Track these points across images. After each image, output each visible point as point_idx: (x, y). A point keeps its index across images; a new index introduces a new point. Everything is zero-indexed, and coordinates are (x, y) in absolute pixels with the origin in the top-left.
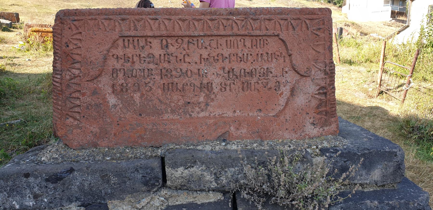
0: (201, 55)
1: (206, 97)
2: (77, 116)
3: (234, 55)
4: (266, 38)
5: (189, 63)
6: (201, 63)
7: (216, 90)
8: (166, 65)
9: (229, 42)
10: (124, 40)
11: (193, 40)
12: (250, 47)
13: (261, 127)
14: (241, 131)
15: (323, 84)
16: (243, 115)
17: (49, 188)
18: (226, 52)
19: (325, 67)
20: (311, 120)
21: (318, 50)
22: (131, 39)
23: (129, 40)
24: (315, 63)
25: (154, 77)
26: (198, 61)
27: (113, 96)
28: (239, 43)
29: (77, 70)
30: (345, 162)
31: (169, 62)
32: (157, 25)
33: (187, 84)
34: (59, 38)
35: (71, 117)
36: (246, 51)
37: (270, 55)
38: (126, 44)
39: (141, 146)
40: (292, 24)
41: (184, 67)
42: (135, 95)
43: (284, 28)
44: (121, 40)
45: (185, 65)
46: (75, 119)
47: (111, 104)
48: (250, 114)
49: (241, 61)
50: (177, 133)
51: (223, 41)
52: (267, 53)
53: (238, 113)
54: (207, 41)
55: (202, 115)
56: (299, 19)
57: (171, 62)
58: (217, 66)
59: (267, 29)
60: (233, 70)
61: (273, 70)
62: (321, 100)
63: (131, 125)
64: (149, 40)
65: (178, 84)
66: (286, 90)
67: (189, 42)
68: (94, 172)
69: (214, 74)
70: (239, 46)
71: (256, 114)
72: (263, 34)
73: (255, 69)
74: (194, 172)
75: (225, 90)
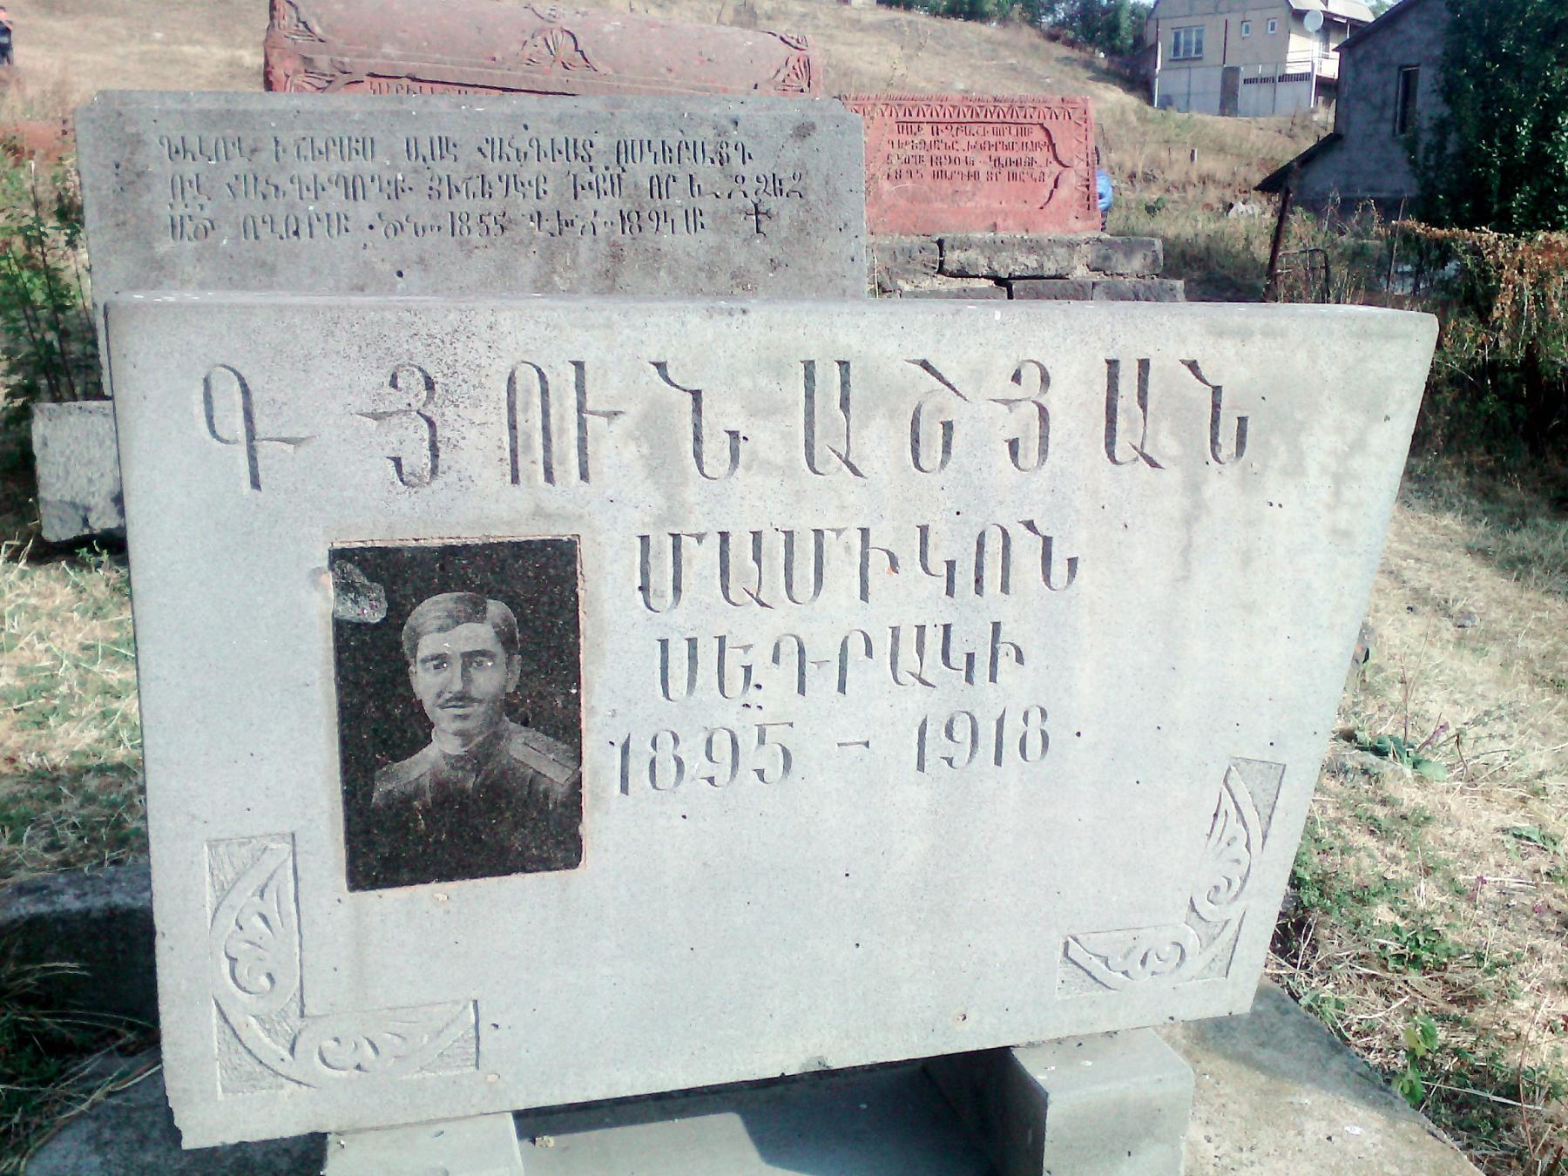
18: (993, 139)
41: (953, 154)
51: (989, 128)
54: (975, 127)
55: (969, 205)
66: (1050, 182)
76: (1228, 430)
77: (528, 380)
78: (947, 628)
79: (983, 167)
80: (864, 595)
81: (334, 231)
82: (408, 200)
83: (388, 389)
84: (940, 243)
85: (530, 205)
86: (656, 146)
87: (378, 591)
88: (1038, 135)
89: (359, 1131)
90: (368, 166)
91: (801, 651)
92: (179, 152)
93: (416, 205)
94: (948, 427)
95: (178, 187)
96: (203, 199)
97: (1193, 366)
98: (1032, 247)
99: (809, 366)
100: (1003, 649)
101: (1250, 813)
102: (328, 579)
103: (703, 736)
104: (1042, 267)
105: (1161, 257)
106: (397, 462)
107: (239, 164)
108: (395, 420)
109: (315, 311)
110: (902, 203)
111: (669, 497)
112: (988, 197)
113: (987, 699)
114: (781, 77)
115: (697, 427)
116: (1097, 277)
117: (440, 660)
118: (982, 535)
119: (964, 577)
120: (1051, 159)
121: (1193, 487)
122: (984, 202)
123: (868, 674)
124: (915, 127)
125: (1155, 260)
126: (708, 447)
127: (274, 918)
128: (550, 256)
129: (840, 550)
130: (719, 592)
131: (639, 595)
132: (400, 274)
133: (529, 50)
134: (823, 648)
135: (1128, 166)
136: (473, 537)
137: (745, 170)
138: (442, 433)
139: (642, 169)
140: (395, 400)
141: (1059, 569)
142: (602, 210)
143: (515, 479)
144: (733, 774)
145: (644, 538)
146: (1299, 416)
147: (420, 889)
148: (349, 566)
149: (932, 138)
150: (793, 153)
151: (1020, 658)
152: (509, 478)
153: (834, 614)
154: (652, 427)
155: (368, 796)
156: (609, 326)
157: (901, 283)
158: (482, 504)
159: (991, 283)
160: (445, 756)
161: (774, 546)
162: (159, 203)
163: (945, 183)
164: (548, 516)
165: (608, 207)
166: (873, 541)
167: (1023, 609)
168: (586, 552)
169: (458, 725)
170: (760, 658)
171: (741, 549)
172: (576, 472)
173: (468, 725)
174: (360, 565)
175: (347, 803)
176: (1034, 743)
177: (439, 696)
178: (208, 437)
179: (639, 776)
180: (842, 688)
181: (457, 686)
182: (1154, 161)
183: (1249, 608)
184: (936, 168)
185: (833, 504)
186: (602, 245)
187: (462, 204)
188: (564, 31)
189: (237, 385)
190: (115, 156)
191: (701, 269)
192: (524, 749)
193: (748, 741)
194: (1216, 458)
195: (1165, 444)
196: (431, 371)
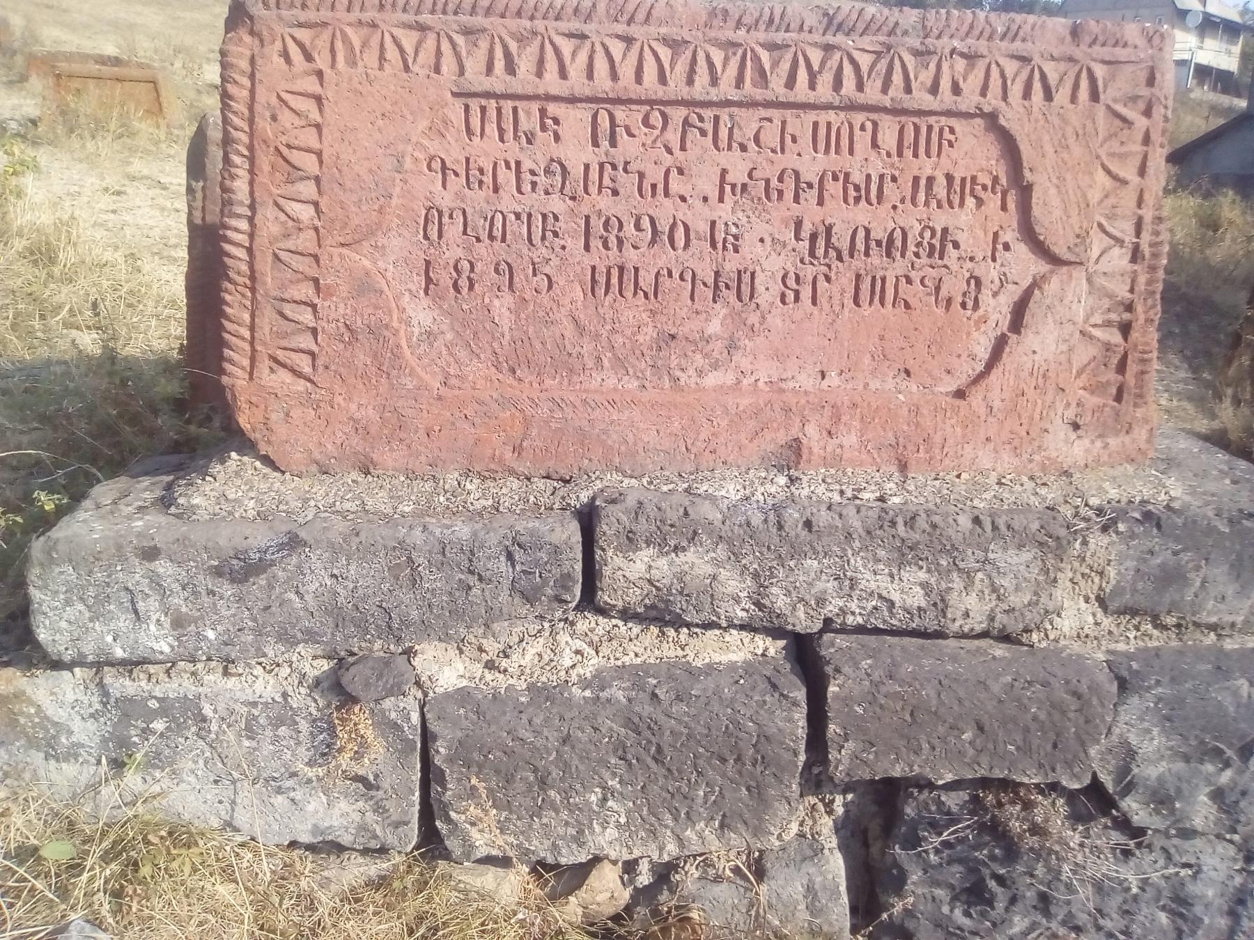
0: (724, 172)
1: (729, 321)
2: (302, 364)
3: (835, 178)
4: (953, 122)
5: (683, 199)
6: (721, 200)
7: (763, 297)
8: (605, 202)
9: (822, 131)
10: (467, 108)
11: (701, 119)
12: (894, 151)
13: (905, 428)
14: (838, 441)
15: (1123, 292)
16: (850, 386)
17: (221, 598)
18: (811, 165)
19: (1138, 235)
20: (1070, 414)
21: (1122, 174)
22: (493, 104)
23: (483, 109)
24: (1108, 217)
25: (562, 242)
26: (714, 195)
27: (426, 302)
28: (857, 132)
29: (304, 206)
30: (1175, 553)
31: (615, 193)
32: (583, 57)
33: (670, 274)
34: (242, 86)
35: (284, 366)
36: (876, 167)
37: (957, 182)
38: (476, 122)
39: (512, 472)
40: (1043, 77)
41: (665, 211)
42: (496, 302)
43: (1016, 90)
44: (458, 105)
45: (667, 202)
46: (297, 373)
47: (416, 331)
48: (874, 384)
49: (857, 200)
50: (630, 438)
51: (801, 124)
52: (949, 178)
53: (833, 379)
54: (749, 122)
55: (712, 379)
56: (1071, 59)
57: (622, 191)
58: (774, 214)
59: (956, 90)
60: (829, 230)
61: (961, 237)
62: (1108, 347)
63: (481, 403)
64: (552, 108)
65: (641, 273)
66: (997, 309)
67: (686, 123)
68: (367, 552)
69: (762, 240)
70: (857, 146)
71: (890, 384)
72: (945, 107)
73: (903, 229)
74: (686, 568)
75: (797, 299)
84: (588, 519)
88: (974, 153)
110: (477, 370)
112: (778, 356)
116: (1131, 640)
120: (1009, 236)
122: (766, 371)
124: (529, 122)
149: (590, 156)
163: (632, 311)
184: (600, 258)
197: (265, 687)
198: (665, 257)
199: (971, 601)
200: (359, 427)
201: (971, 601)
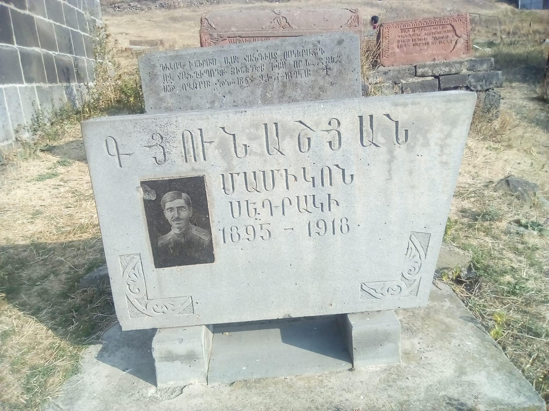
8: (414, 37)
18: (434, 31)
36: (440, 30)
41: (420, 37)
54: (427, 28)
66: (454, 43)
76: (402, 134)
77: (187, 134)
78: (314, 196)
79: (430, 40)
80: (288, 188)
81: (206, 86)
82: (226, 76)
83: (152, 140)
85: (259, 74)
86: (296, 52)
87: (153, 192)
88: (449, 28)
89: (165, 328)
90: (214, 67)
91: (270, 204)
92: (165, 68)
93: (228, 77)
94: (309, 139)
95: (165, 77)
96: (171, 81)
97: (388, 116)
98: (447, 65)
99: (266, 125)
100: (332, 202)
101: (419, 248)
102: (141, 189)
103: (245, 228)
104: (450, 71)
105: (494, 63)
106: (155, 158)
107: (180, 70)
108: (154, 147)
109: (131, 121)
110: (403, 55)
111: (228, 164)
113: (328, 216)
114: (349, 23)
115: (235, 144)
116: (470, 73)
117: (171, 209)
118: (322, 169)
119: (318, 181)
120: (454, 35)
121: (391, 152)
123: (291, 210)
125: (492, 64)
126: (238, 149)
127: (138, 275)
128: (265, 87)
129: (279, 176)
130: (245, 188)
131: (223, 190)
132: (224, 97)
133: (272, 24)
134: (277, 202)
135: (507, 30)
136: (176, 176)
137: (322, 56)
138: (166, 150)
139: (291, 60)
140: (154, 143)
141: (348, 179)
142: (280, 73)
143: (186, 161)
144: (254, 238)
145: (223, 175)
146: (426, 128)
147: (174, 268)
148: (146, 186)
150: (337, 49)
151: (338, 204)
152: (185, 161)
153: (279, 193)
154: (222, 146)
155: (157, 244)
156: (208, 118)
157: (402, 81)
158: (179, 168)
159: (433, 78)
160: (176, 234)
161: (260, 175)
162: (160, 82)
163: (417, 47)
164: (196, 170)
165: (280, 72)
166: (288, 173)
167: (337, 190)
168: (207, 179)
169: (178, 226)
170: (259, 206)
171: (250, 177)
172: (203, 158)
173: (181, 225)
174: (148, 185)
175: (152, 246)
176: (345, 228)
177: (172, 218)
178: (108, 154)
179: (228, 239)
180: (283, 214)
181: (176, 216)
182: (517, 28)
183: (413, 187)
184: (414, 42)
185: (275, 162)
186: (280, 83)
187: (241, 75)
188: (283, 17)
189: (114, 141)
190: (148, 71)
191: (309, 87)
192: (195, 231)
193: (258, 228)
194: (398, 143)
195: (380, 139)
196: (161, 134)
197: (387, 84)
198: (420, 42)
199: (453, 70)
200: (392, 62)
201: (453, 70)
